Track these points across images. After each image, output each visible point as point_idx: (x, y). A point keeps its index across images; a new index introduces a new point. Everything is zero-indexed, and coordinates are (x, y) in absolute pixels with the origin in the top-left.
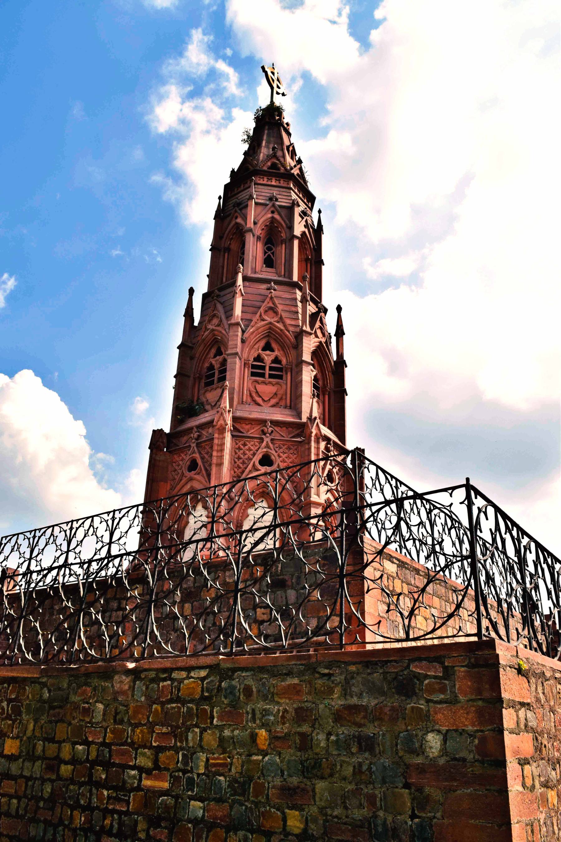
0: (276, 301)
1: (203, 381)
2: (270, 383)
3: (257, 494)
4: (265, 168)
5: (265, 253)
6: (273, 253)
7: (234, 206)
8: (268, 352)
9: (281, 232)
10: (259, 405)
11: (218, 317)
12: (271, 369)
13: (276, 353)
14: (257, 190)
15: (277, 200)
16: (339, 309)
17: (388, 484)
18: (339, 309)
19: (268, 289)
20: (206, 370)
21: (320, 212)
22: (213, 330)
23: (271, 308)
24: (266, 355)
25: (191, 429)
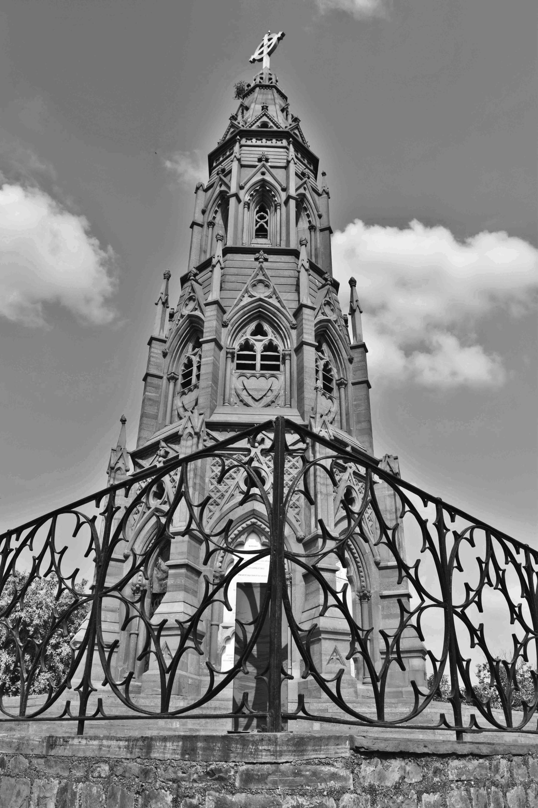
0: (269, 273)
1: (180, 381)
2: (263, 376)
3: (244, 529)
4: (254, 128)
5: (257, 222)
6: (266, 222)
7: (218, 174)
8: (259, 337)
9: (274, 196)
10: (247, 405)
11: (194, 300)
12: (263, 358)
13: (269, 337)
14: (242, 152)
15: (267, 160)
16: (352, 283)
17: (409, 517)
18: (352, 283)
19: (257, 259)
20: (183, 368)
21: (324, 174)
22: (189, 316)
23: (260, 281)
24: (256, 340)
25: (158, 443)
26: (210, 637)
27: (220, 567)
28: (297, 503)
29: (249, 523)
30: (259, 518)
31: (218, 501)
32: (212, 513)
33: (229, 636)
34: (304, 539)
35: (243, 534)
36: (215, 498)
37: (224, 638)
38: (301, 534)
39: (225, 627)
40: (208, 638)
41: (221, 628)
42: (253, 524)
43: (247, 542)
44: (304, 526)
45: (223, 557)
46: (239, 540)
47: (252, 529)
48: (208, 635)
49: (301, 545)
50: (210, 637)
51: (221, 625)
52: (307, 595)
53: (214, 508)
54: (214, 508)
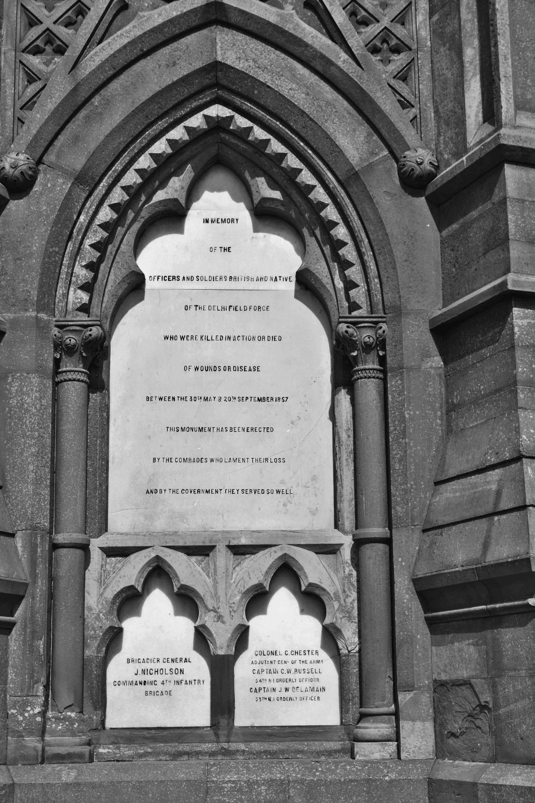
26: (51, 596)
27: (85, 308)
28: (399, 31)
29: (196, 121)
30: (238, 101)
31: (62, 31)
32: (38, 85)
33: (132, 587)
34: (431, 176)
35: (177, 172)
36: (48, 23)
37: (110, 594)
38: (420, 156)
39: (110, 552)
40: (40, 604)
41: (96, 555)
42: (217, 126)
43: (195, 205)
44: (432, 124)
45: (93, 267)
46: (160, 196)
47: (213, 151)
48: (41, 587)
49: (423, 200)
50: (51, 596)
51: (96, 544)
52: (451, 409)
53: (47, 63)
54: (47, 63)
